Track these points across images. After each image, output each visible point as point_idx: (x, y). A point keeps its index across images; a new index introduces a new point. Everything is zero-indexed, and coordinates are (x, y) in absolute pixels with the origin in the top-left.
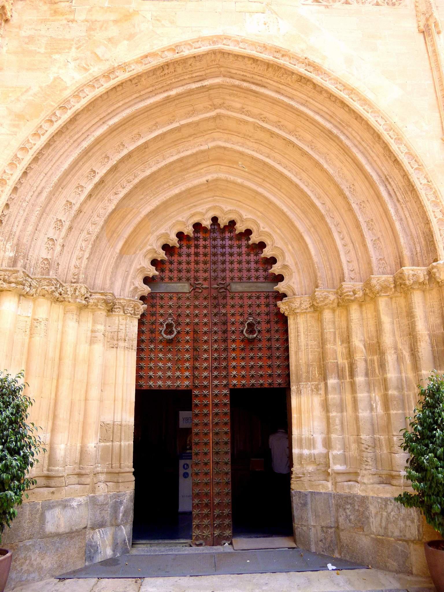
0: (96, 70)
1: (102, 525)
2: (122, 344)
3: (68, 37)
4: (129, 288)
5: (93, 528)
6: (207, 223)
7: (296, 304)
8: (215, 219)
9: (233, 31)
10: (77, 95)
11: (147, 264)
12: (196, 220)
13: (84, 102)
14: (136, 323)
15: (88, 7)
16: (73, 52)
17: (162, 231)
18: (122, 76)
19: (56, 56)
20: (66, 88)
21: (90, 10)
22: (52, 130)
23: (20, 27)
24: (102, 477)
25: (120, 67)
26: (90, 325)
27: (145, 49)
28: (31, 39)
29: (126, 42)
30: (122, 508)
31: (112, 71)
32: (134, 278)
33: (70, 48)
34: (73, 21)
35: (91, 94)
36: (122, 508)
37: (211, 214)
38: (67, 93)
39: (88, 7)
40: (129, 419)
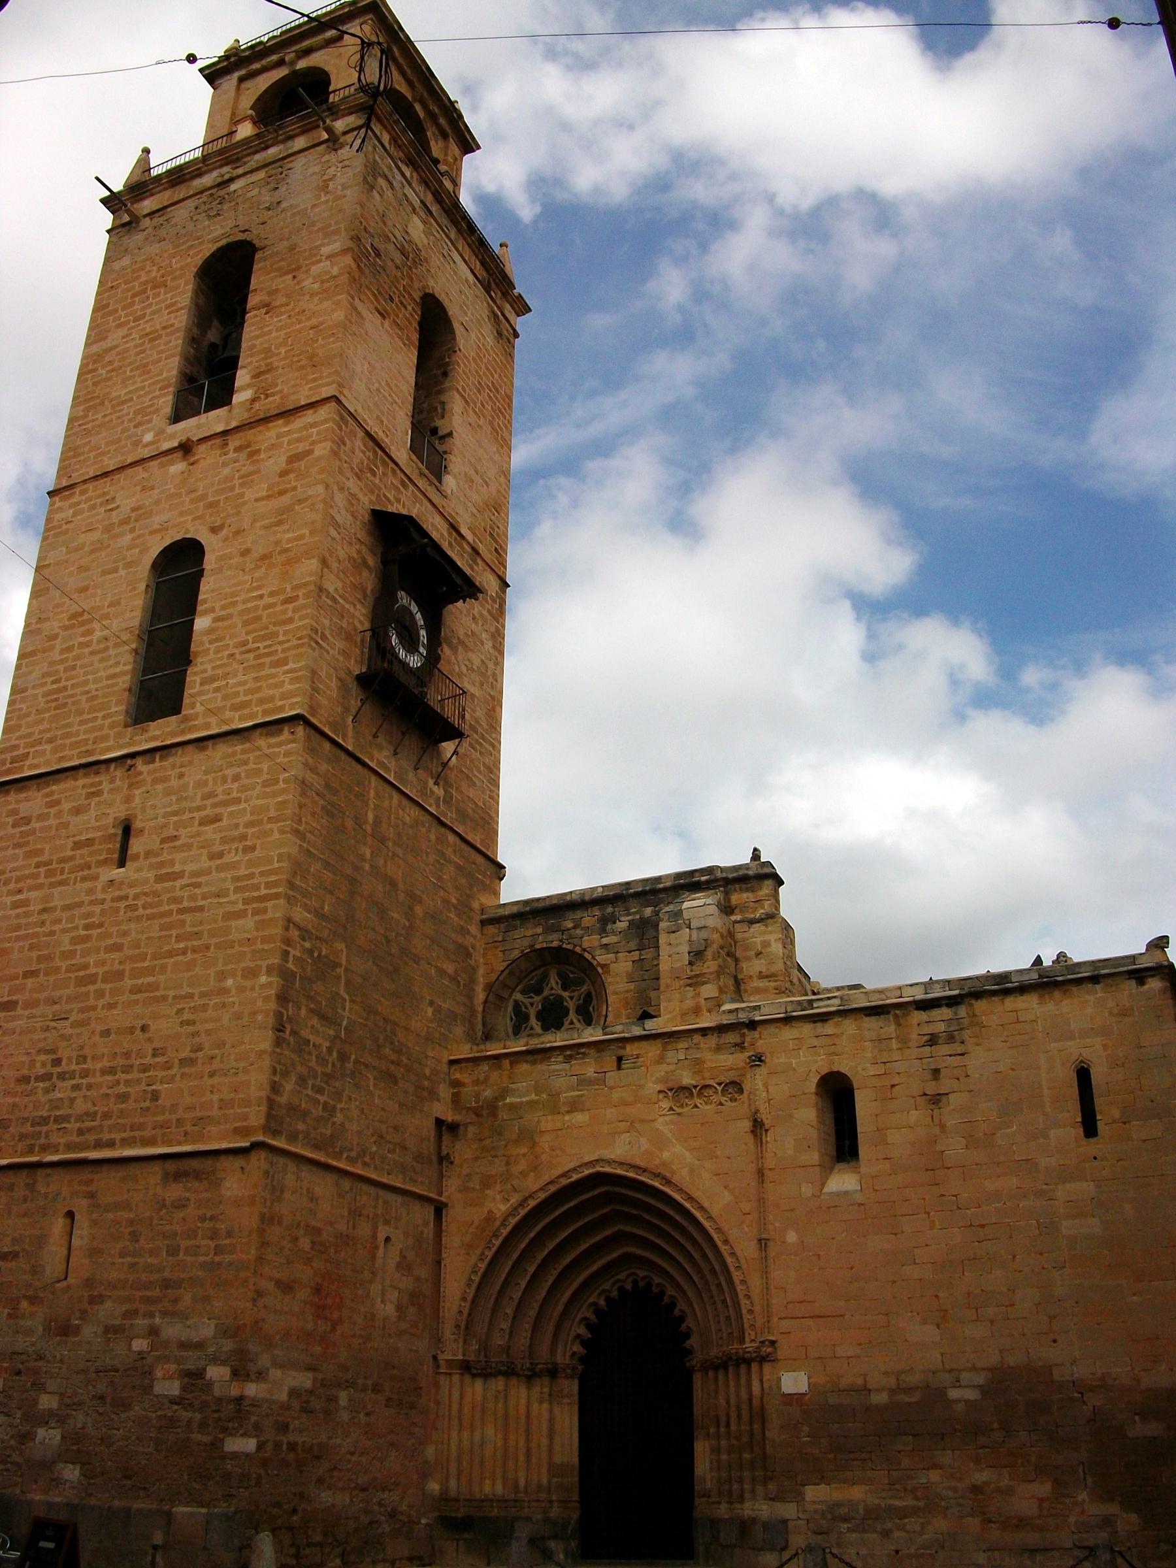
0: (515, 1199)
1: (555, 1537)
2: (566, 1400)
3: (493, 1173)
4: (568, 1354)
5: (549, 1539)
6: (629, 1286)
7: (694, 1363)
8: (635, 1282)
9: (608, 1154)
10: (503, 1224)
11: (582, 1330)
12: (619, 1284)
13: (509, 1228)
14: (576, 1381)
15: (503, 1143)
16: (498, 1187)
17: (591, 1300)
18: (532, 1203)
19: (488, 1192)
20: (495, 1220)
21: (506, 1146)
22: (490, 1254)
23: (461, 1166)
24: (556, 1504)
25: (530, 1196)
26: (539, 1388)
27: (546, 1178)
28: (469, 1176)
29: (532, 1174)
30: (570, 1528)
31: (525, 1200)
32: (572, 1344)
33: (495, 1183)
34: (495, 1156)
35: (513, 1221)
36: (570, 1528)
37: (630, 1280)
38: (498, 1223)
39: (503, 1143)
40: (575, 1460)
